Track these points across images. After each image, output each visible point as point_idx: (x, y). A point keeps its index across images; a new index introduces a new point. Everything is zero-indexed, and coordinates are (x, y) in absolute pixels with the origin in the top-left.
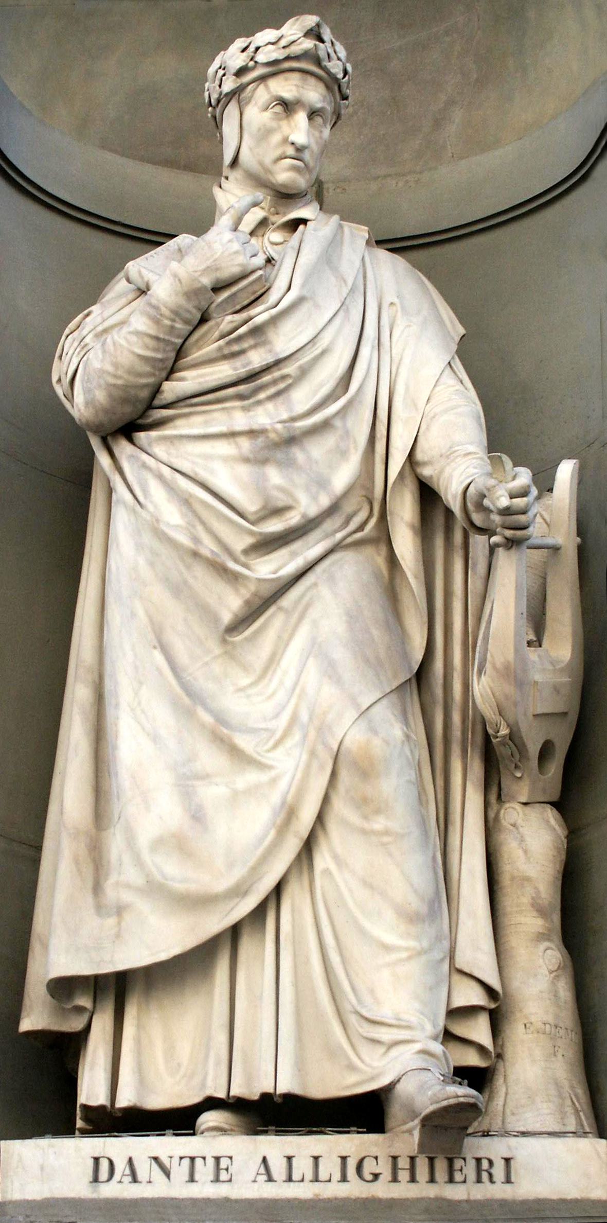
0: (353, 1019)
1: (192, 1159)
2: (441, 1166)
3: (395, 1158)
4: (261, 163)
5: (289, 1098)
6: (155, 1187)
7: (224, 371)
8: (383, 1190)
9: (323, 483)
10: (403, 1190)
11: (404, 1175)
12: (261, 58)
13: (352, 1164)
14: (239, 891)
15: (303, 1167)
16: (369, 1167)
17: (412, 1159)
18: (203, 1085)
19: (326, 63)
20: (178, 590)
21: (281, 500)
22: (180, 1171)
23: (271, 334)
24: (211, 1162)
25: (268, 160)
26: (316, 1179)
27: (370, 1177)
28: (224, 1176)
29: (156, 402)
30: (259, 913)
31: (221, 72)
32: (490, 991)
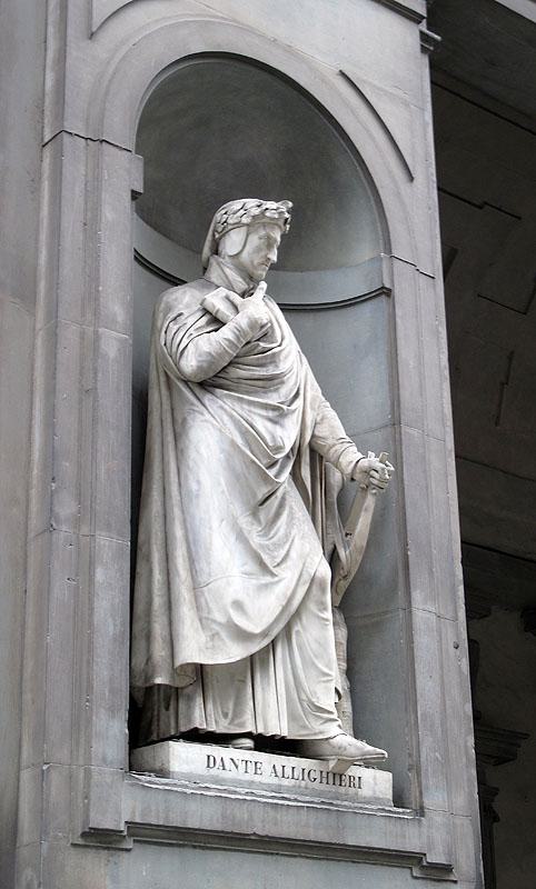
4: (252, 262)
6: (231, 773)
8: (316, 785)
11: (324, 780)
12: (268, 214)
13: (306, 772)
14: (264, 634)
15: (288, 772)
25: (255, 262)
28: (259, 772)
31: (242, 212)
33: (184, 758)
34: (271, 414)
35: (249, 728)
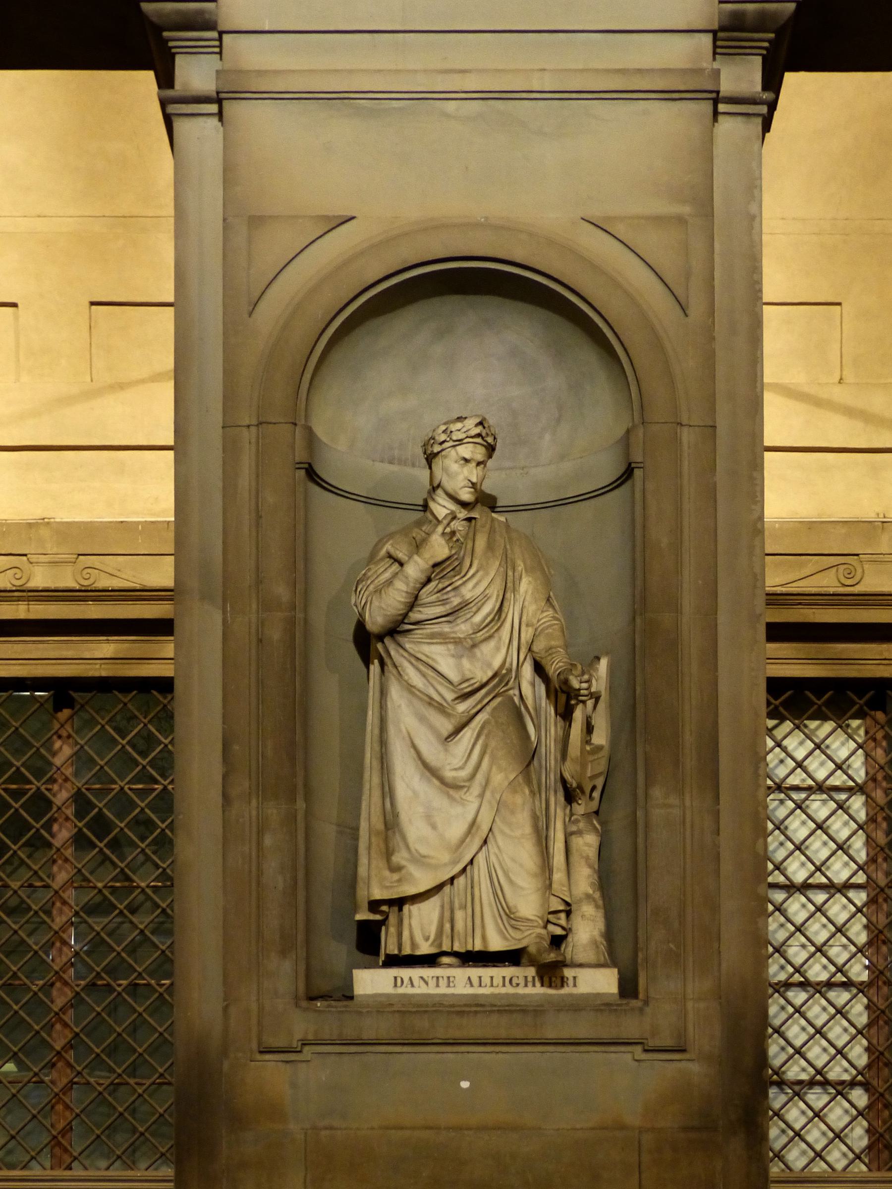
1: (438, 978)
2: (546, 979)
3: (526, 977)
5: (480, 953)
6: (420, 989)
7: (439, 610)
8: (521, 990)
9: (489, 665)
10: (530, 990)
11: (530, 984)
15: (486, 980)
16: (515, 981)
18: (440, 945)
20: (422, 719)
21: (468, 675)
22: (432, 983)
24: (446, 979)
26: (492, 986)
28: (451, 984)
29: (406, 621)
30: (464, 870)
32: (567, 904)
33: (372, 982)
35: (446, 947)
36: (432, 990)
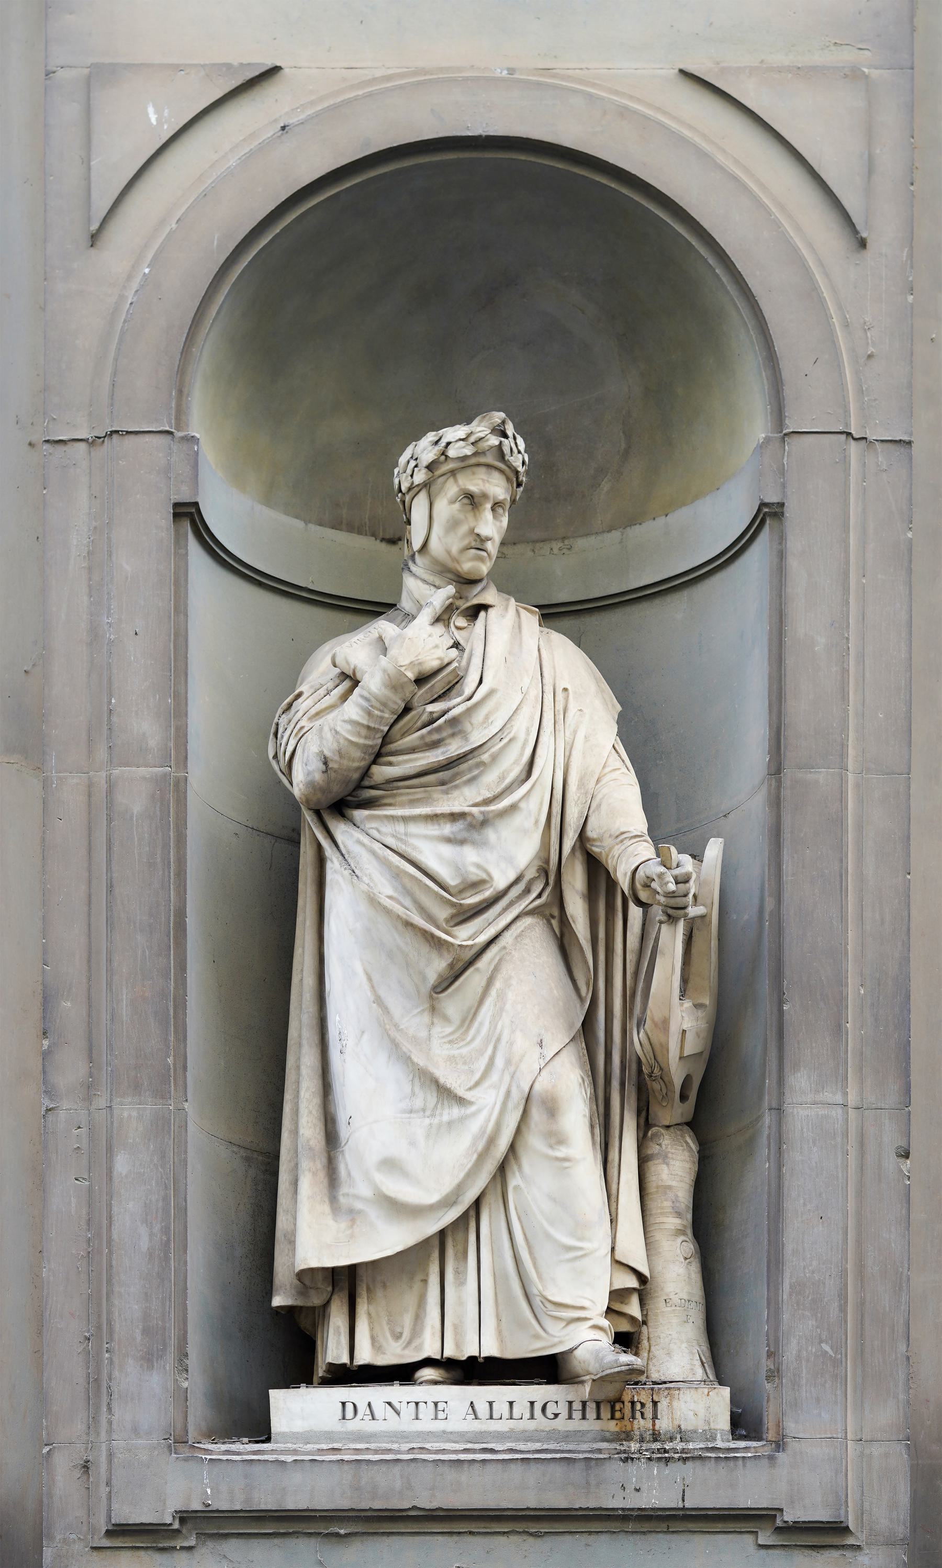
0: (537, 1301)
3: (570, 1403)
5: (489, 1359)
8: (561, 1424)
11: (577, 1415)
14: (448, 1202)
15: (501, 1408)
16: (550, 1410)
17: (584, 1404)
19: (507, 458)
22: (408, 1412)
23: (467, 726)
27: (552, 1416)
28: (441, 1415)
31: (413, 463)
34: (448, 829)
35: (430, 1350)
36: (405, 1423)
